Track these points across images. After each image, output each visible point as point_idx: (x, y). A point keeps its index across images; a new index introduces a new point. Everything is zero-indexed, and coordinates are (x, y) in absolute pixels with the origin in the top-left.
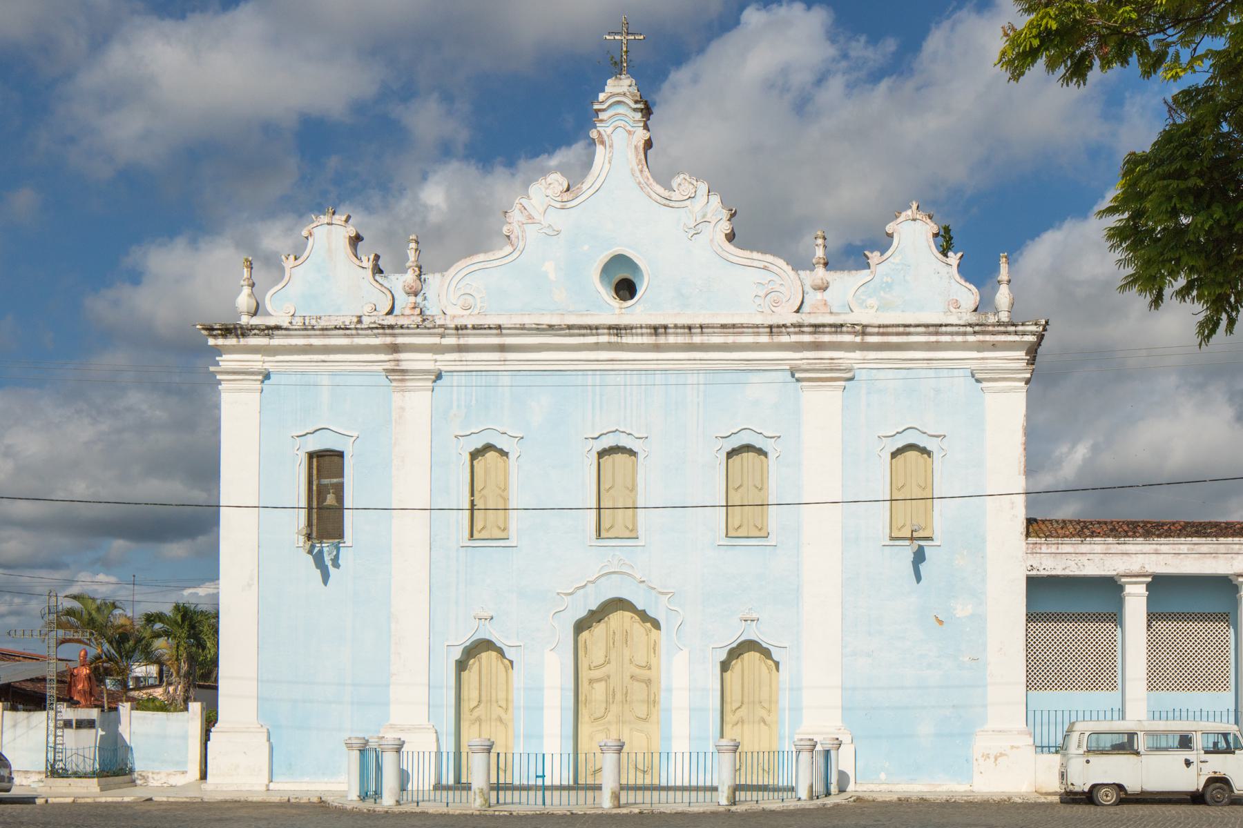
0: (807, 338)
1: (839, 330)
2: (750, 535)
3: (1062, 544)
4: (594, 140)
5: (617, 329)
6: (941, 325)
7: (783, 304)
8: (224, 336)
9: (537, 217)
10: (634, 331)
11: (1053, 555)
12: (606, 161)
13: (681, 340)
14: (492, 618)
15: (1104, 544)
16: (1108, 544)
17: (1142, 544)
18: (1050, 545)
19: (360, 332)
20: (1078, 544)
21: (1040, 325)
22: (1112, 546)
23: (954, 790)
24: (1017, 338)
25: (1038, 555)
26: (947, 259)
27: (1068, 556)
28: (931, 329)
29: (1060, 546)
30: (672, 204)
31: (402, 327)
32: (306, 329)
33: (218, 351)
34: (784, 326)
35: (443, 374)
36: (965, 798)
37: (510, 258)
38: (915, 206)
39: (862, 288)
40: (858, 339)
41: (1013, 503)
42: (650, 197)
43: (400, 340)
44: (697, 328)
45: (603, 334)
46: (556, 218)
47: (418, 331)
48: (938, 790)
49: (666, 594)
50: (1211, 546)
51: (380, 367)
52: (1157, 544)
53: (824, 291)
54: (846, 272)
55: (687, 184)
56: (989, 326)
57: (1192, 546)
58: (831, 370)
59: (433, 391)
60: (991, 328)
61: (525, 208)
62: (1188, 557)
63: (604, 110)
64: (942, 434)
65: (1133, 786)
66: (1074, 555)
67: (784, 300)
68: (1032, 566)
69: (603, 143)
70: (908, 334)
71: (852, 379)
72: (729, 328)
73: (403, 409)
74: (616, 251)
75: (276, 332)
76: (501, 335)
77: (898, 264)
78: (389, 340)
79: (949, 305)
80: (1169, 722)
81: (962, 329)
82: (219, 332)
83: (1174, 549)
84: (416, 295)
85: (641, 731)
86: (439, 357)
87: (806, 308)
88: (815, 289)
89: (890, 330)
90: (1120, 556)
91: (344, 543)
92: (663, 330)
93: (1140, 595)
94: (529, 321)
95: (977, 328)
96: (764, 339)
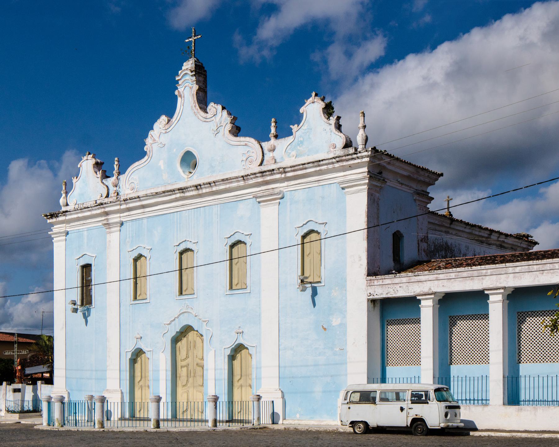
0: (260, 180)
1: (273, 172)
2: (242, 288)
3: (385, 279)
4: (177, 95)
5: (182, 190)
6: (320, 161)
7: (254, 163)
8: (52, 218)
9: (157, 139)
10: (188, 189)
11: (381, 286)
12: (182, 105)
13: (208, 190)
14: (141, 338)
15: (407, 277)
16: (410, 276)
17: (428, 275)
18: (379, 280)
19: (93, 208)
20: (393, 278)
21: (369, 151)
22: (412, 278)
23: (329, 424)
24: (359, 161)
25: (373, 286)
26: (329, 122)
27: (389, 286)
28: (316, 164)
29: (384, 280)
30: (207, 120)
31: (105, 203)
32: (75, 210)
33: (52, 225)
34: (248, 175)
35: (124, 222)
36: (316, 429)
37: (147, 162)
38: (313, 94)
39: (289, 147)
40: (283, 176)
41: (360, 257)
42: (199, 119)
43: (107, 209)
44: (212, 183)
45: (177, 193)
46: (164, 139)
47: (111, 204)
48: (322, 424)
49: (205, 321)
50: (469, 272)
51: (100, 224)
52: (437, 274)
53: (274, 151)
54: (283, 139)
55: (213, 109)
56: (343, 157)
57: (457, 274)
58: (272, 195)
59: (120, 231)
60: (344, 158)
61: (152, 136)
62: (456, 280)
63: (180, 79)
64: (325, 222)
65: (373, 423)
66: (392, 285)
67: (254, 160)
68: (370, 293)
69: (180, 96)
70: (306, 168)
71: (282, 198)
72: (225, 181)
73: (110, 241)
74: (186, 150)
75: (67, 213)
76: (140, 201)
77: (306, 129)
78: (103, 210)
79: (330, 147)
80: (404, 384)
81: (331, 161)
82: (49, 217)
84: (116, 187)
85: (200, 392)
86: (122, 215)
87: (265, 163)
88: (269, 151)
89: (296, 168)
90: (417, 284)
91: (92, 306)
92: (200, 187)
93: (429, 307)
94: (149, 192)
95: (337, 159)
96: (242, 183)
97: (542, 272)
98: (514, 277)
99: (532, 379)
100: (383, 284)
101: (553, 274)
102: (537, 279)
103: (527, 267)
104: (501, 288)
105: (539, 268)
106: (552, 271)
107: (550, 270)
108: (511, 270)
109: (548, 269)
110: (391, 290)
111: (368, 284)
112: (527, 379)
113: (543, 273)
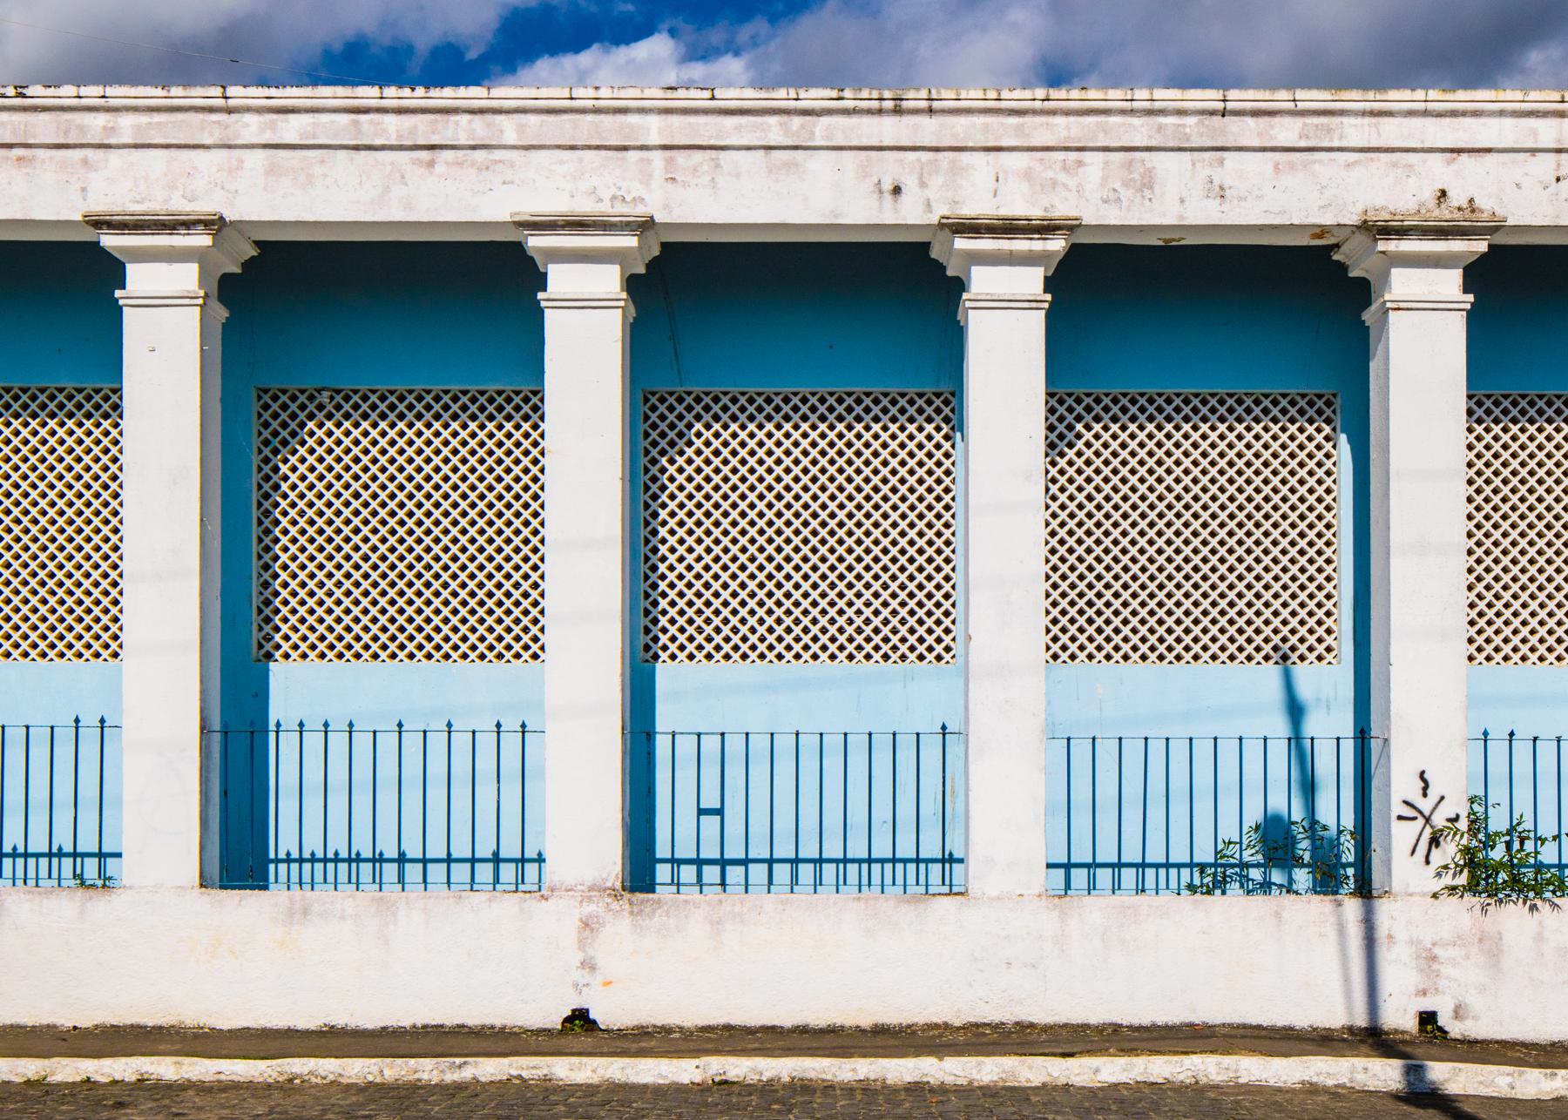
97: (424, 155)
98: (272, 171)
99: (362, 742)
101: (484, 172)
103: (344, 119)
104: (199, 222)
105: (413, 131)
106: (480, 155)
107: (474, 147)
108: (254, 128)
109: (463, 142)
112: (338, 741)
113: (431, 164)
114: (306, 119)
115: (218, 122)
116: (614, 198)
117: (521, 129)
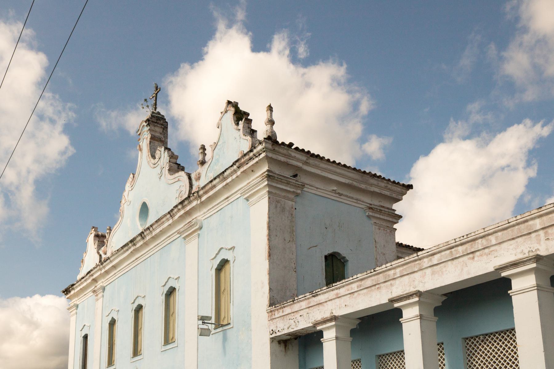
6: (223, 172)
15: (306, 299)
22: (311, 300)
24: (257, 160)
29: (284, 309)
50: (373, 278)
52: (337, 289)
60: (243, 160)
62: (359, 294)
66: (292, 314)
68: (272, 330)
71: (201, 228)
83: (348, 290)
95: (237, 164)
97: (471, 256)
98: (433, 273)
100: (283, 315)
101: (489, 256)
102: (465, 269)
103: (448, 252)
104: (413, 294)
105: (466, 249)
106: (487, 251)
107: (484, 249)
108: (426, 262)
109: (480, 248)
110: (292, 321)
111: (270, 317)
113: (473, 258)
114: (439, 255)
115: (418, 263)
116: (529, 251)
117: (497, 238)
